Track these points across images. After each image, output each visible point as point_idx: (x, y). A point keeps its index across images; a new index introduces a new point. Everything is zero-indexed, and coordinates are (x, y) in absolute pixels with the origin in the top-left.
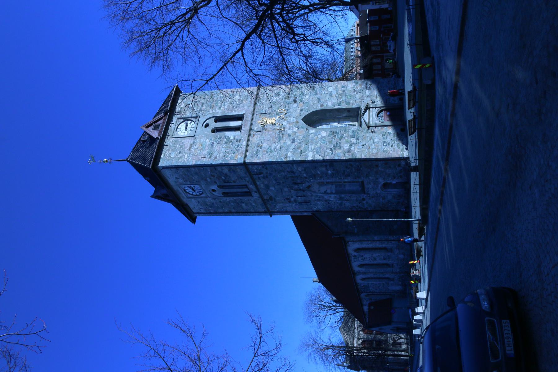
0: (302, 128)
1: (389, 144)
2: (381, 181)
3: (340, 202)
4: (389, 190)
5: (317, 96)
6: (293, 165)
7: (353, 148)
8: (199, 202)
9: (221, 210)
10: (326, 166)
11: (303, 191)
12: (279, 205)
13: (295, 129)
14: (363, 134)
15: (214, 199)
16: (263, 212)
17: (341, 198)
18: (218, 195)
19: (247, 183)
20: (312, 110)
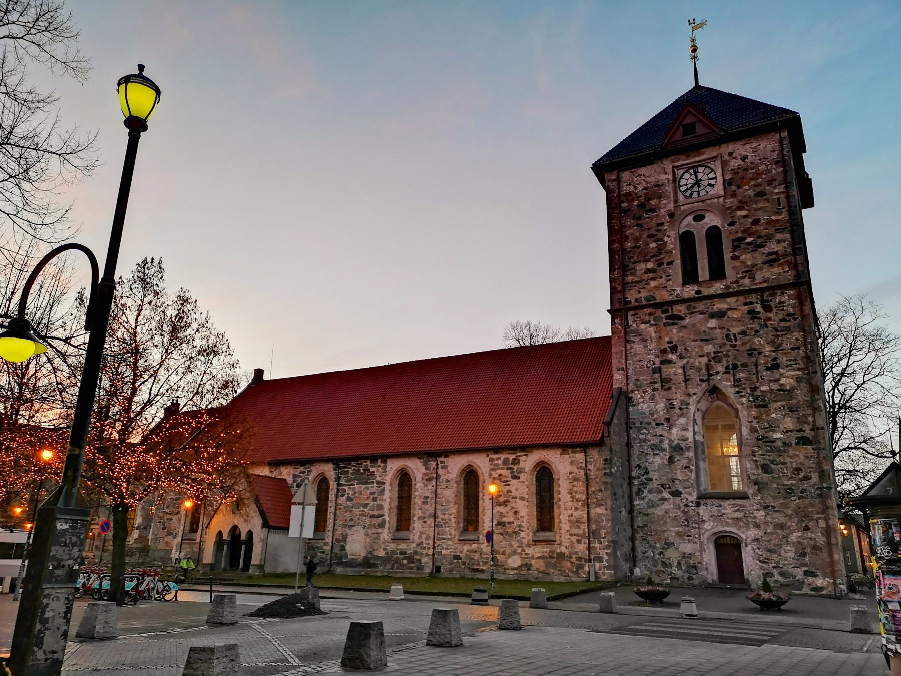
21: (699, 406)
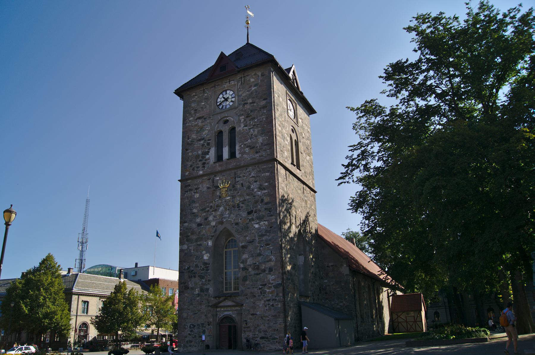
0: (216, 230)
1: (191, 331)
13: (213, 224)
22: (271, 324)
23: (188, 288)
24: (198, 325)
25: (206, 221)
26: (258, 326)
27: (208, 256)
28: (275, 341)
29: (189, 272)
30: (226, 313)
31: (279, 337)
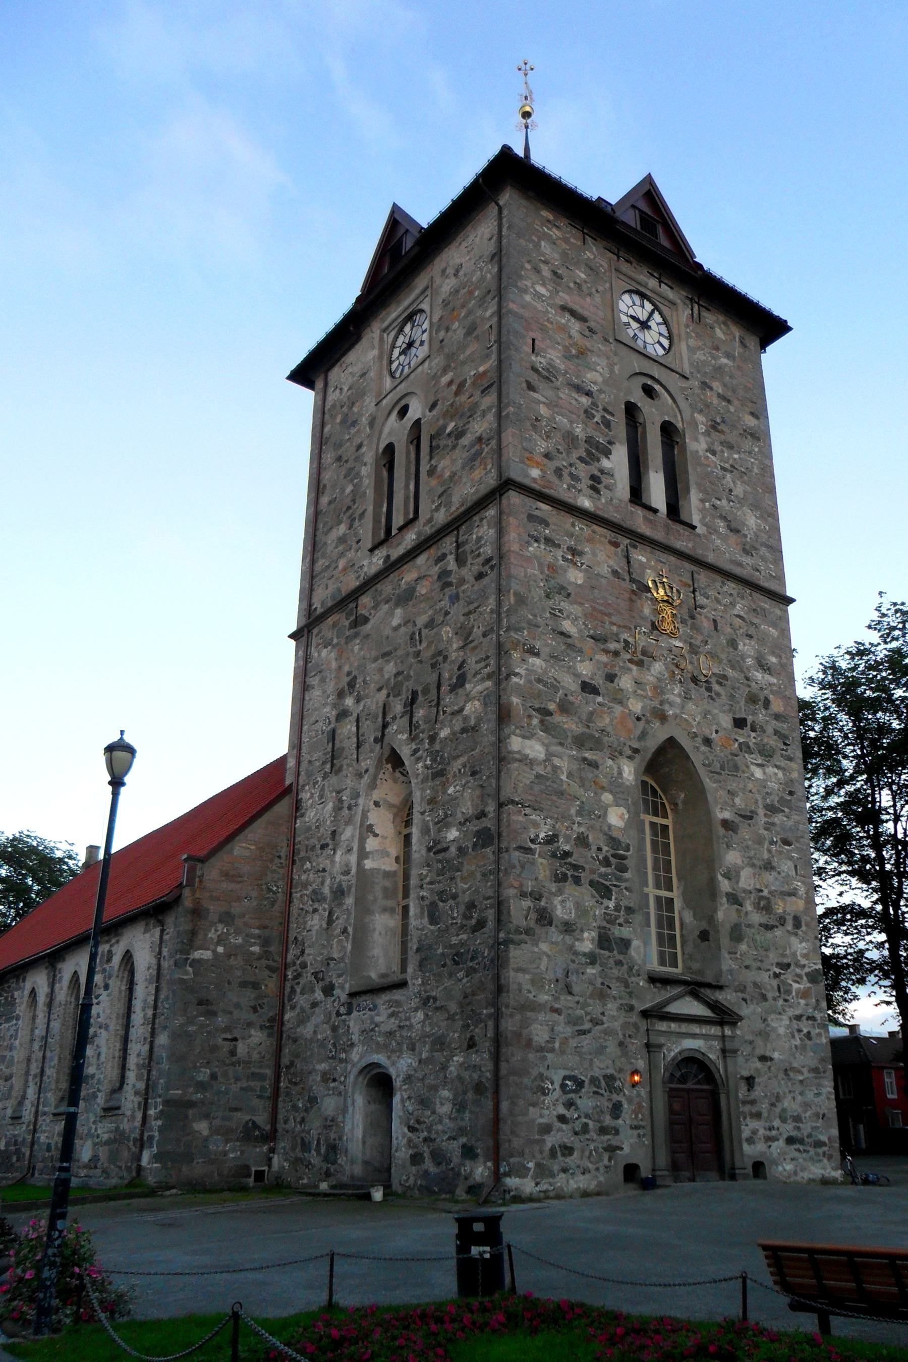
0: (643, 736)
2: (400, 1067)
3: (326, 891)
4: (360, 1100)
5: (761, 811)
6: (489, 676)
7: (554, 934)
8: (363, 375)
9: (329, 457)
10: (482, 815)
11: (380, 740)
12: (333, 655)
13: (636, 706)
14: (616, 989)
15: (371, 424)
16: (310, 605)
17: (339, 893)
18: (386, 430)
19: (424, 515)
20: (709, 783)
21: (376, 795)
22: (810, 1095)
23: (550, 924)
24: (594, 1081)
25: (609, 684)
26: (778, 1098)
27: (621, 817)
28: (820, 1150)
29: (554, 855)
30: (689, 1044)
31: (829, 1139)
